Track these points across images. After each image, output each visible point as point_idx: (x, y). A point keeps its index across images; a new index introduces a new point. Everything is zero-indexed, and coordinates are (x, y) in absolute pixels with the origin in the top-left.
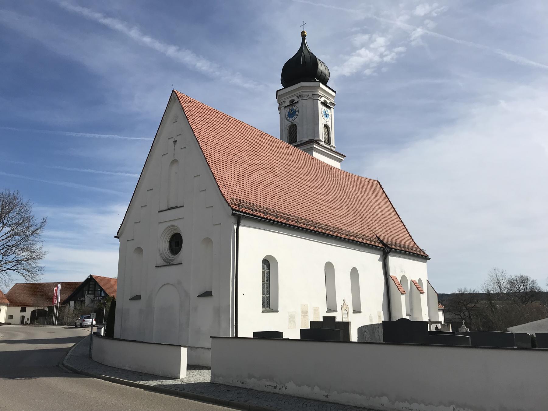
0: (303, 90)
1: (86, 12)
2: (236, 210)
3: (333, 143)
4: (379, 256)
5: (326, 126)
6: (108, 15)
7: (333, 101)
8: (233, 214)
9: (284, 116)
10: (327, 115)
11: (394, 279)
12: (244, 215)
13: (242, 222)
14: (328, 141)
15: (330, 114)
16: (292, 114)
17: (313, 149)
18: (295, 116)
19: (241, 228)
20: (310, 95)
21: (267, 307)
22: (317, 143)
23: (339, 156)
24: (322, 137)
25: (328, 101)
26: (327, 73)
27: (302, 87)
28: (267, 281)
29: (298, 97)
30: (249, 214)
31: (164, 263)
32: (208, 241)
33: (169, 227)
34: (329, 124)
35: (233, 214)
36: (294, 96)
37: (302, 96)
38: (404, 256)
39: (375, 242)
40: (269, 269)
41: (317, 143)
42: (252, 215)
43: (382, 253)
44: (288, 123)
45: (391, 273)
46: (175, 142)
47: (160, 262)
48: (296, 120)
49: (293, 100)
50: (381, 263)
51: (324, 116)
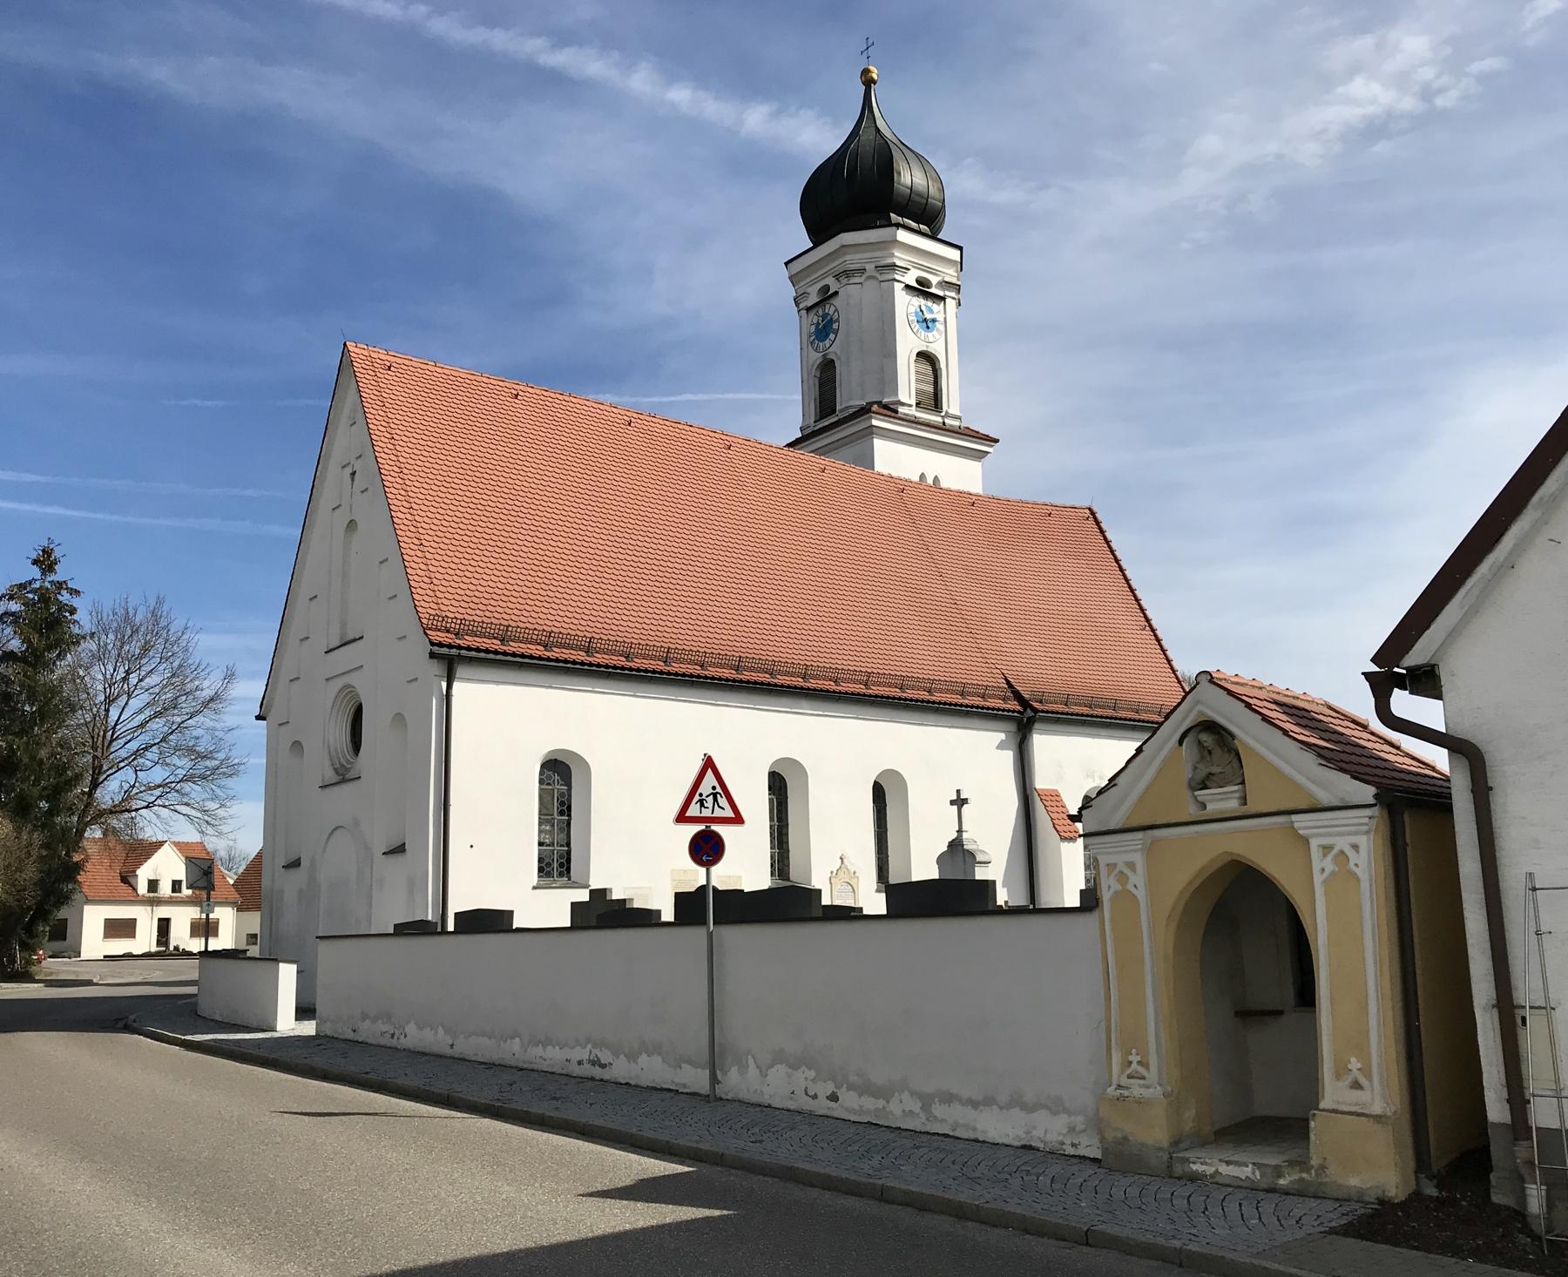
0: (847, 257)
2: (440, 645)
3: (953, 402)
4: (1002, 736)
5: (926, 357)
7: (951, 275)
8: (432, 655)
9: (805, 338)
10: (927, 324)
11: (1053, 797)
12: (455, 656)
13: (461, 671)
14: (934, 401)
15: (940, 317)
16: (824, 330)
17: (871, 431)
18: (832, 336)
19: (456, 685)
20: (870, 267)
21: (561, 875)
22: (890, 410)
23: (973, 441)
24: (907, 389)
25: (934, 280)
26: (933, 191)
27: (844, 248)
28: (561, 813)
29: (837, 277)
30: (496, 652)
31: (335, 779)
32: (399, 719)
33: (341, 690)
34: (937, 349)
35: (432, 655)
36: (823, 277)
37: (847, 274)
38: (1103, 732)
39: (1005, 699)
40: (569, 785)
41: (890, 410)
42: (505, 654)
43: (1012, 727)
44: (816, 358)
45: (1041, 782)
46: (353, 474)
47: (331, 776)
48: (835, 348)
49: (827, 288)
50: (1008, 757)
51: (916, 327)
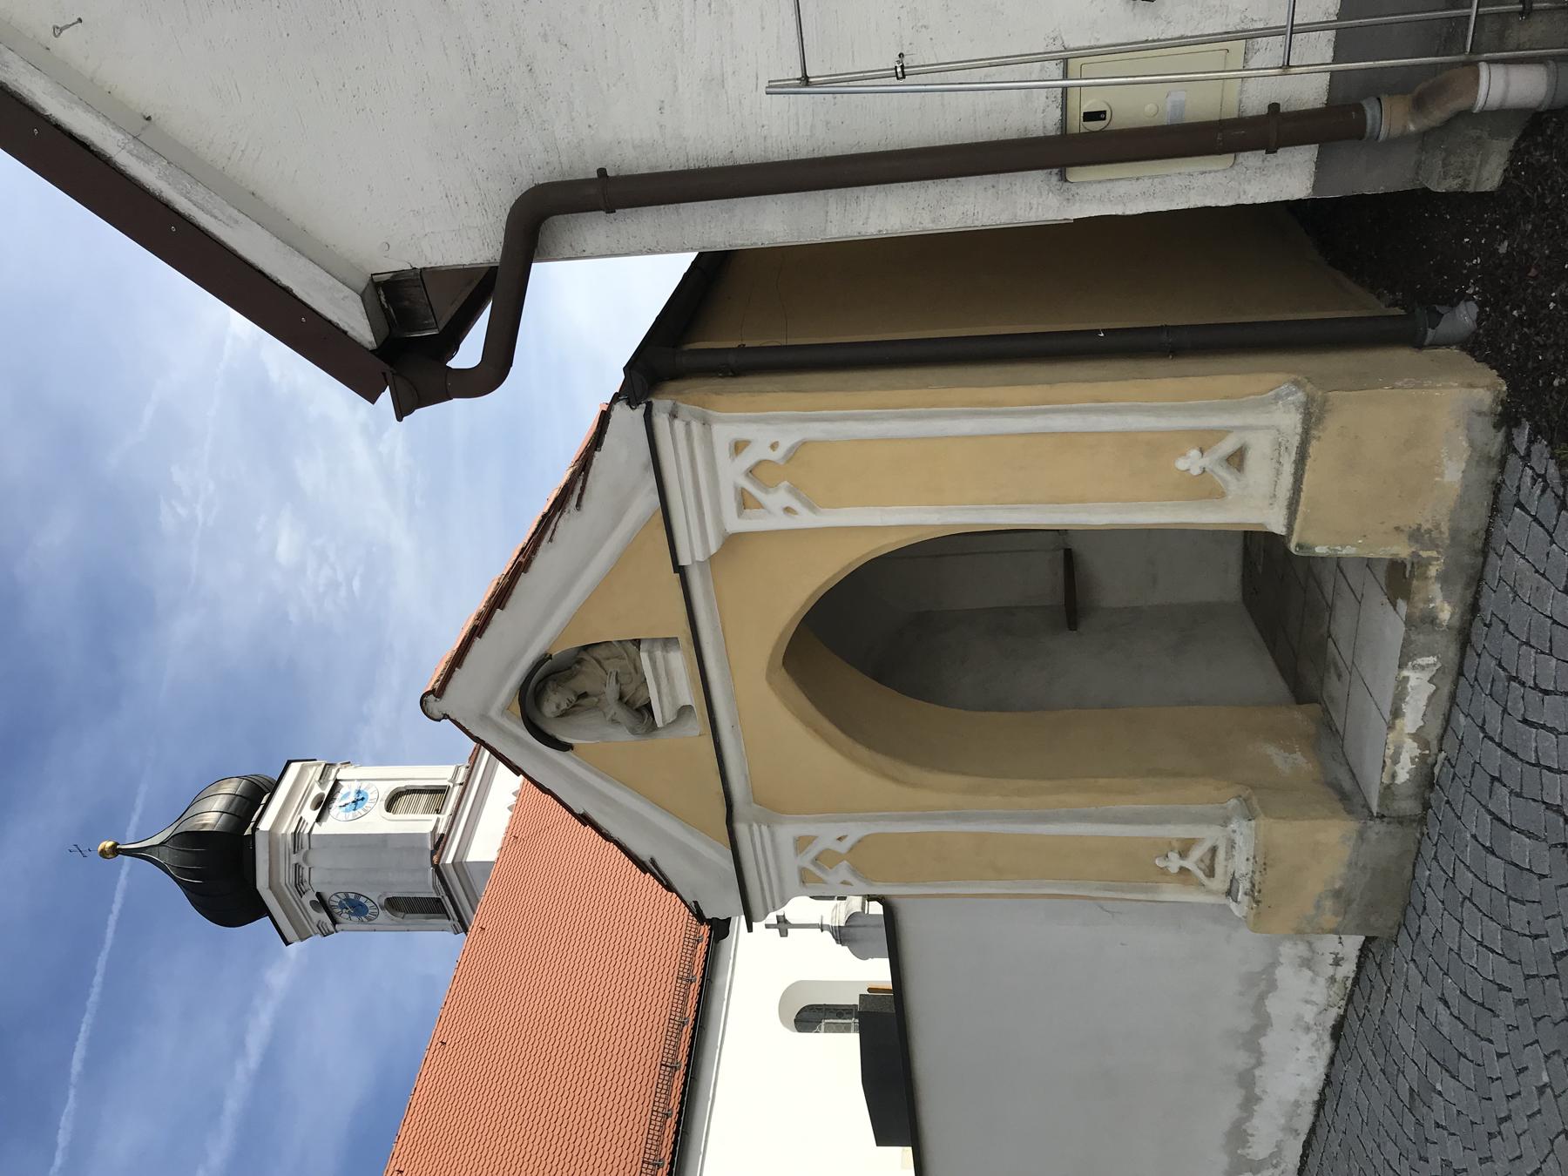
0: (282, 881)
1: (232, 1105)
6: (239, 1046)
7: (314, 772)
10: (359, 800)
15: (355, 786)
16: (356, 907)
17: (459, 865)
18: (362, 900)
20: (295, 859)
22: (440, 842)
24: (418, 822)
25: (317, 791)
29: (301, 893)
34: (386, 789)
37: (299, 885)
41: (440, 842)
44: (384, 916)
48: (375, 896)
49: (312, 903)
51: (360, 811)
